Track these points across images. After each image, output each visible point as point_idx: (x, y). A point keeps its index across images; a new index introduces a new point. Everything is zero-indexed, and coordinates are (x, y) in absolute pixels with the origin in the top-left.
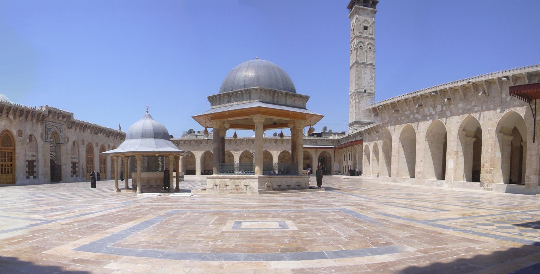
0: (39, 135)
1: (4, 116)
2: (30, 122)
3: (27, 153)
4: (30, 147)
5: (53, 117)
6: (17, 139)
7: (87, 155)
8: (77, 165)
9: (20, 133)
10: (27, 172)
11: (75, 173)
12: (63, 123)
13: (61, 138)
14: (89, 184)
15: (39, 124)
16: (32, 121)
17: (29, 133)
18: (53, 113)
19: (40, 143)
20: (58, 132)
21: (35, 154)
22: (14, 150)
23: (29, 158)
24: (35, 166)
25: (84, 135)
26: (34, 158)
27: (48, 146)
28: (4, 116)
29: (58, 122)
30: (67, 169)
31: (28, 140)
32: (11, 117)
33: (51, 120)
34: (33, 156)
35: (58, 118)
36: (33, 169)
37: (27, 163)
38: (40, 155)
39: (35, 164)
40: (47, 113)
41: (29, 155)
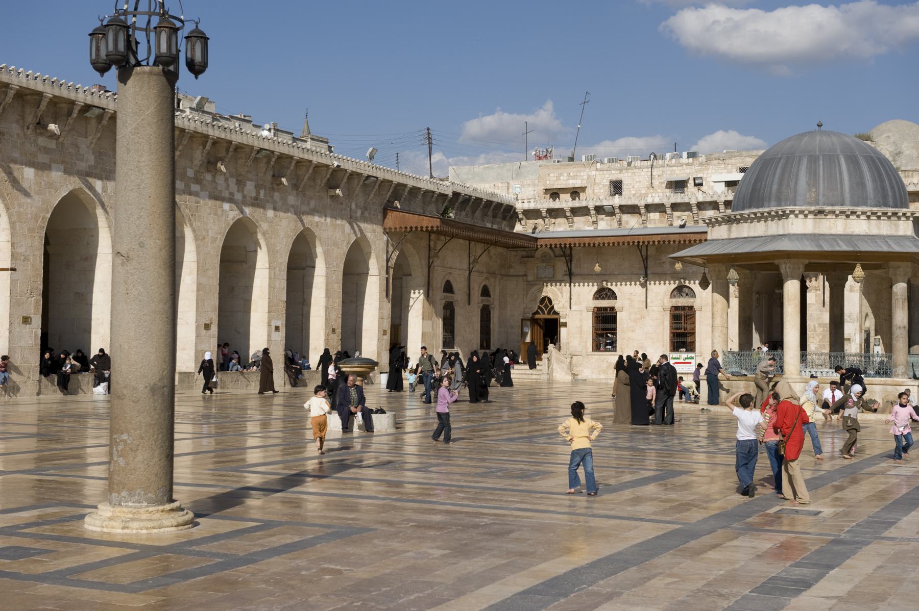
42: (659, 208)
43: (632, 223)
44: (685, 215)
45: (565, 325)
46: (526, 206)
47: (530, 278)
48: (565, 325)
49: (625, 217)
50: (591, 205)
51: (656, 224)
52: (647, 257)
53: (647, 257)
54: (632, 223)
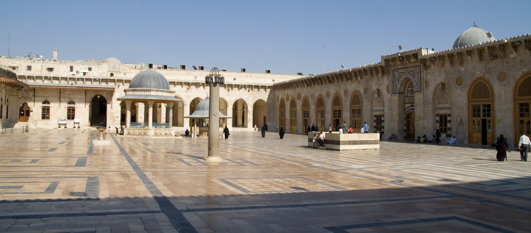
0: (385, 88)
1: (354, 79)
2: (376, 78)
3: (375, 108)
4: (379, 102)
5: (402, 63)
6: (364, 96)
7: (469, 101)
8: (449, 118)
9: (366, 90)
10: (375, 127)
11: (446, 131)
13: (415, 84)
14: (494, 153)
17: (374, 87)
18: (389, 61)
19: (386, 96)
20: (411, 77)
21: (382, 108)
22: (362, 107)
23: (377, 113)
25: (462, 69)
26: (382, 113)
27: (396, 97)
28: (354, 79)
29: (411, 65)
30: (425, 124)
31: (376, 96)
32: (359, 78)
34: (380, 111)
35: (409, 62)
36: (381, 124)
37: (375, 118)
38: (386, 109)
39: (382, 119)
40: (383, 64)
41: (377, 111)
42: (65, 79)
43: (56, 83)
44: (73, 82)
45: (32, 111)
46: (20, 74)
47: (20, 96)
48: (32, 111)
49: (54, 81)
50: (43, 76)
51: (63, 83)
52: (61, 93)
53: (61, 93)
54: (56, 83)
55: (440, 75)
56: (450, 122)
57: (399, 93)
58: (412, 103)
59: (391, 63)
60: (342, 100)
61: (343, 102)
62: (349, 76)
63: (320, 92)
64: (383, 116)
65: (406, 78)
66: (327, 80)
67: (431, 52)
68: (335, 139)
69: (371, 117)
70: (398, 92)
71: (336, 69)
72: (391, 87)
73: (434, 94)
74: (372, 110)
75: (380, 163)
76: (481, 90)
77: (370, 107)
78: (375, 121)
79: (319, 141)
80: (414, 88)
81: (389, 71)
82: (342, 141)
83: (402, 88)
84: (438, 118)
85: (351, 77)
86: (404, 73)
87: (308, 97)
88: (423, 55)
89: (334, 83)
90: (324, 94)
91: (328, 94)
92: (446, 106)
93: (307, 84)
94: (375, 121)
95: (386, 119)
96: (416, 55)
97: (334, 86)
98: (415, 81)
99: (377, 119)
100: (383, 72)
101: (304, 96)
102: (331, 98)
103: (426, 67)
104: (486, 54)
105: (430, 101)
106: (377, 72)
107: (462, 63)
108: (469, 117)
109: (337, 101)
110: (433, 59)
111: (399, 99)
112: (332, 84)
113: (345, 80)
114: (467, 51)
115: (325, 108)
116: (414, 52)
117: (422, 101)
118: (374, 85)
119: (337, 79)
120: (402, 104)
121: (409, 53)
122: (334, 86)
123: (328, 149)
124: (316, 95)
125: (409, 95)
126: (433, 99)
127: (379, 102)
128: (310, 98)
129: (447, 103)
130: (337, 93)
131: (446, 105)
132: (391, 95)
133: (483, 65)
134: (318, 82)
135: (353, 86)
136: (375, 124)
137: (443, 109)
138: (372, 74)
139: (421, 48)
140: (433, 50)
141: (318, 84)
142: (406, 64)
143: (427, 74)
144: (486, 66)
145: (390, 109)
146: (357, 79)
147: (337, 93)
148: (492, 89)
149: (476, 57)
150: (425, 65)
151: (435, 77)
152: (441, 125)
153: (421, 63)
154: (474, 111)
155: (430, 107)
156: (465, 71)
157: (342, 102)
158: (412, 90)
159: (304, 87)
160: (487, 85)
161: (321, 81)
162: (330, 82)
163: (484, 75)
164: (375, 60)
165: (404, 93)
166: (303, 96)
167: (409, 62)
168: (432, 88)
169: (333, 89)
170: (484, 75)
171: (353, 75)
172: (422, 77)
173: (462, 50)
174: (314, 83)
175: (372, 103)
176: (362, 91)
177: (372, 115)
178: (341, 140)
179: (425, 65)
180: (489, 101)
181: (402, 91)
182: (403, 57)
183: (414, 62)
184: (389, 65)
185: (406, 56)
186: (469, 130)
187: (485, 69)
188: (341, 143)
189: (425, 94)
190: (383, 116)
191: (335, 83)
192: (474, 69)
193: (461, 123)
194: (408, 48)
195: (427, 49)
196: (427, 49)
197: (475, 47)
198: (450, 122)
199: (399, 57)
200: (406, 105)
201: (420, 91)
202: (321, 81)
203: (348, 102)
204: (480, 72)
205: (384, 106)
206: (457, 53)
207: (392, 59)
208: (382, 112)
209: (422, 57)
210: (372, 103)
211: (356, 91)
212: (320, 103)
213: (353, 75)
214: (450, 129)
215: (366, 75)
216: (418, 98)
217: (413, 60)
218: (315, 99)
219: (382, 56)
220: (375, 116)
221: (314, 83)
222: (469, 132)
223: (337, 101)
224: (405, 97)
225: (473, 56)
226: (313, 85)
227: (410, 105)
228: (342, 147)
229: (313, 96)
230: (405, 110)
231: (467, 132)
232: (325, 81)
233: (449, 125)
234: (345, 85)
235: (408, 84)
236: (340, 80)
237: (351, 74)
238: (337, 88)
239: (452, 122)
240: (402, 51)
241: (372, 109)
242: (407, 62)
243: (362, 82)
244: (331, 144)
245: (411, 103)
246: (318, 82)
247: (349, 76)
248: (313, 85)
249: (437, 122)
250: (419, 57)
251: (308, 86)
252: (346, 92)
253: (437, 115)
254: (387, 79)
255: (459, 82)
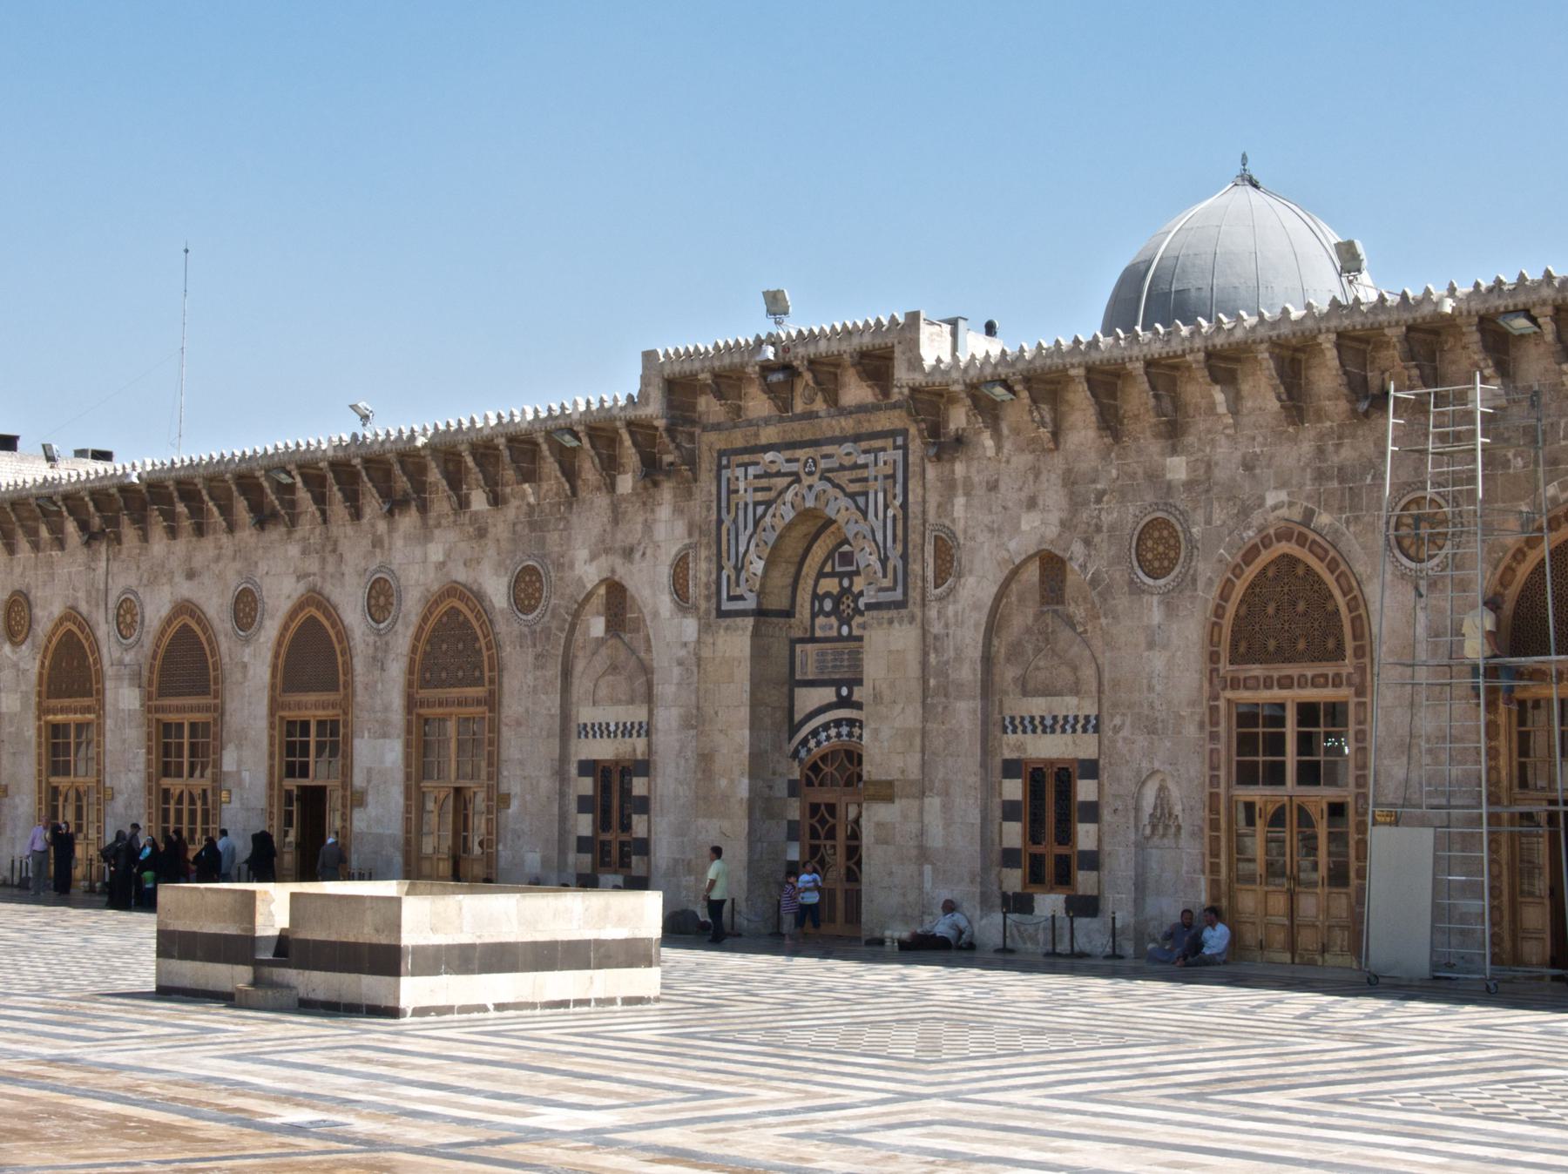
0: (664, 573)
2: (602, 501)
3: (586, 714)
4: (614, 668)
6: (507, 628)
8: (1085, 790)
9: (527, 587)
10: (583, 844)
11: (1064, 878)
12: (883, 421)
13: (867, 557)
15: (666, 492)
16: (612, 487)
17: (588, 572)
19: (670, 629)
20: (839, 508)
21: (640, 714)
23: (602, 750)
24: (643, 805)
25: (1177, 468)
27: (736, 643)
28: (441, 504)
29: (847, 425)
30: (932, 824)
33: (769, 435)
34: (627, 731)
35: (832, 400)
36: (626, 827)
37: (586, 786)
38: (667, 718)
41: (602, 730)
55: (1032, 504)
56: (1091, 812)
57: (760, 613)
58: (846, 683)
59: (709, 407)
60: (347, 652)
61: (359, 665)
62: (402, 483)
63: (186, 590)
64: (644, 767)
65: (804, 515)
66: (241, 506)
67: (977, 346)
68: (366, 933)
69: (561, 775)
70: (750, 603)
71: (323, 431)
72: (701, 569)
73: (994, 626)
74: (566, 727)
75: (706, 1094)
76: (1288, 611)
77: (552, 702)
78: (584, 804)
79: (239, 948)
80: (859, 584)
81: (692, 461)
82: (418, 950)
83: (781, 578)
84: (1014, 789)
85: (420, 486)
86: (798, 480)
87: (85, 624)
88: (929, 361)
89: (293, 522)
90: (215, 605)
91: (246, 608)
92: (1068, 705)
93: (83, 526)
94: (584, 804)
95: (667, 785)
96: (878, 357)
97: (294, 550)
98: (867, 534)
99: (604, 787)
100: (652, 470)
101: (57, 610)
102: (270, 631)
103: (946, 446)
104: (1326, 376)
105: (968, 673)
106: (610, 466)
107: (1173, 431)
108: (1214, 780)
109: (312, 654)
110: (985, 391)
111: (759, 653)
112: (275, 533)
113: (372, 505)
114: (1212, 355)
115: (219, 710)
116: (867, 340)
117: (914, 669)
118: (582, 554)
119: (320, 500)
120: (775, 686)
121: (835, 347)
122: (294, 550)
123: (307, 1006)
124: (156, 608)
125: (826, 626)
126: (988, 660)
127: (614, 668)
128: (104, 630)
129: (1076, 690)
130: (314, 599)
131: (1072, 701)
132: (705, 628)
133: (1307, 448)
134: (170, 516)
135: (436, 552)
136: (584, 825)
137: (1050, 726)
138: (570, 474)
139: (914, 318)
140: (990, 329)
141: (172, 532)
142: (811, 416)
143: (950, 486)
144: (1320, 451)
145: (696, 720)
146: (463, 503)
147: (314, 599)
148: (1357, 603)
149: (1261, 391)
150: (935, 430)
151: (1002, 512)
152: (1034, 833)
153: (914, 414)
154: (1246, 744)
155: (965, 713)
156: (1189, 485)
157: (349, 670)
158: (845, 591)
159: (61, 544)
160: (1329, 579)
161: (197, 511)
162: (263, 518)
163: (1309, 515)
164: (605, 381)
165: (789, 613)
166: (47, 612)
167: (832, 400)
168: (977, 587)
169: (281, 572)
170: (1309, 515)
171: (434, 475)
172: (914, 509)
173: (1175, 346)
174: (141, 522)
175: (567, 673)
176: (497, 590)
177: (564, 758)
178: (409, 939)
179: (935, 430)
180: (1337, 682)
181: (778, 601)
182: (788, 368)
183: (862, 408)
184: (685, 420)
185: (813, 363)
186: (1215, 868)
187: (1320, 476)
188: (407, 963)
189: (936, 628)
190: (644, 767)
191: (304, 528)
192: (1250, 474)
193: (1163, 817)
194: (820, 313)
195: (953, 323)
196: (953, 323)
197: (1263, 332)
198: (1091, 812)
199: (766, 368)
200: (800, 692)
201: (901, 605)
202: (197, 511)
203: (397, 670)
204: (1283, 496)
205: (650, 698)
206: (1150, 364)
207: (717, 376)
208: (640, 744)
209: (919, 379)
210: (567, 673)
211: (453, 590)
212: (185, 662)
213: (434, 475)
214: (1092, 861)
215: (530, 475)
216: (888, 648)
217: (856, 392)
218: (148, 641)
219: (649, 356)
220: (587, 767)
221: (141, 522)
222: (1214, 884)
223: (312, 654)
224: (794, 642)
225: (1245, 387)
226: (129, 533)
227: (828, 695)
228: (412, 990)
229: (127, 616)
230: (794, 729)
231: (1203, 882)
232: (226, 510)
233: (1086, 836)
234: (377, 543)
235: (819, 551)
236: (338, 509)
237: (422, 469)
238: (313, 565)
239: (1106, 814)
240: (790, 328)
241: (566, 716)
242: (819, 405)
243: (501, 525)
244: (344, 975)
245: (838, 684)
246: (170, 516)
247: (402, 483)
248: (129, 533)
249: (1010, 811)
250: (902, 375)
251: (91, 537)
252: (381, 598)
253: (1011, 768)
254: (678, 511)
255: (1158, 548)
